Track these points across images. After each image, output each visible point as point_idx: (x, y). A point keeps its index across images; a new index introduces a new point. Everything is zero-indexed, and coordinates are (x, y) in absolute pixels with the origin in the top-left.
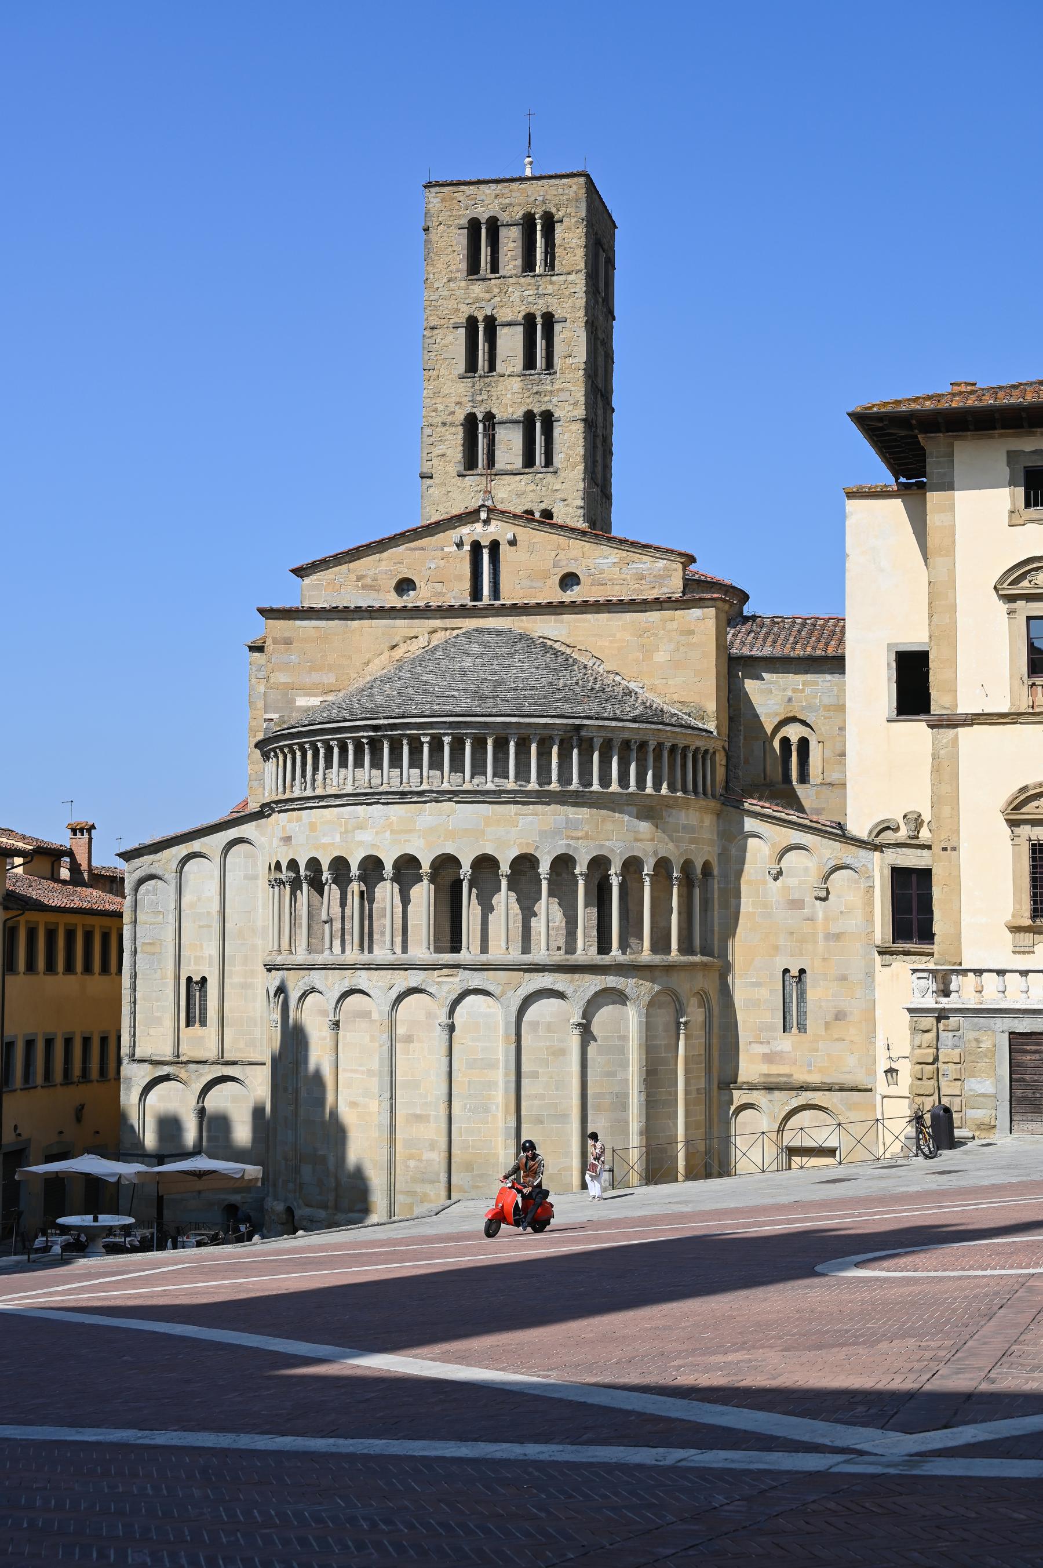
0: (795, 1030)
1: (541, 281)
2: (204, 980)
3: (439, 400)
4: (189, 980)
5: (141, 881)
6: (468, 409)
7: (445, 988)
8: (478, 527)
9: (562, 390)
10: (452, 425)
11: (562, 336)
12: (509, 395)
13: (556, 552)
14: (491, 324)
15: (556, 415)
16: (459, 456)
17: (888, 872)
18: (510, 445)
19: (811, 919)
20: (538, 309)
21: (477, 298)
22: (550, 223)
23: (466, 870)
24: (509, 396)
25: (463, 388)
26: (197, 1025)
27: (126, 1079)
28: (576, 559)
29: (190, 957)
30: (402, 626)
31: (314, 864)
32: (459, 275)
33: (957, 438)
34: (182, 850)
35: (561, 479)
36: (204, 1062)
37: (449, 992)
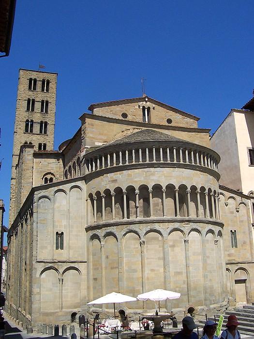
0: (234, 247)
2: (62, 233)
4: (57, 233)
5: (40, 198)
6: (27, 118)
7: (187, 228)
8: (144, 103)
12: (37, 117)
14: (34, 101)
16: (24, 129)
18: (36, 128)
21: (31, 95)
22: (48, 82)
23: (189, 189)
25: (26, 114)
26: (59, 249)
27: (35, 268)
28: (171, 115)
29: (57, 225)
30: (125, 127)
34: (56, 188)
36: (64, 262)
37: (188, 230)
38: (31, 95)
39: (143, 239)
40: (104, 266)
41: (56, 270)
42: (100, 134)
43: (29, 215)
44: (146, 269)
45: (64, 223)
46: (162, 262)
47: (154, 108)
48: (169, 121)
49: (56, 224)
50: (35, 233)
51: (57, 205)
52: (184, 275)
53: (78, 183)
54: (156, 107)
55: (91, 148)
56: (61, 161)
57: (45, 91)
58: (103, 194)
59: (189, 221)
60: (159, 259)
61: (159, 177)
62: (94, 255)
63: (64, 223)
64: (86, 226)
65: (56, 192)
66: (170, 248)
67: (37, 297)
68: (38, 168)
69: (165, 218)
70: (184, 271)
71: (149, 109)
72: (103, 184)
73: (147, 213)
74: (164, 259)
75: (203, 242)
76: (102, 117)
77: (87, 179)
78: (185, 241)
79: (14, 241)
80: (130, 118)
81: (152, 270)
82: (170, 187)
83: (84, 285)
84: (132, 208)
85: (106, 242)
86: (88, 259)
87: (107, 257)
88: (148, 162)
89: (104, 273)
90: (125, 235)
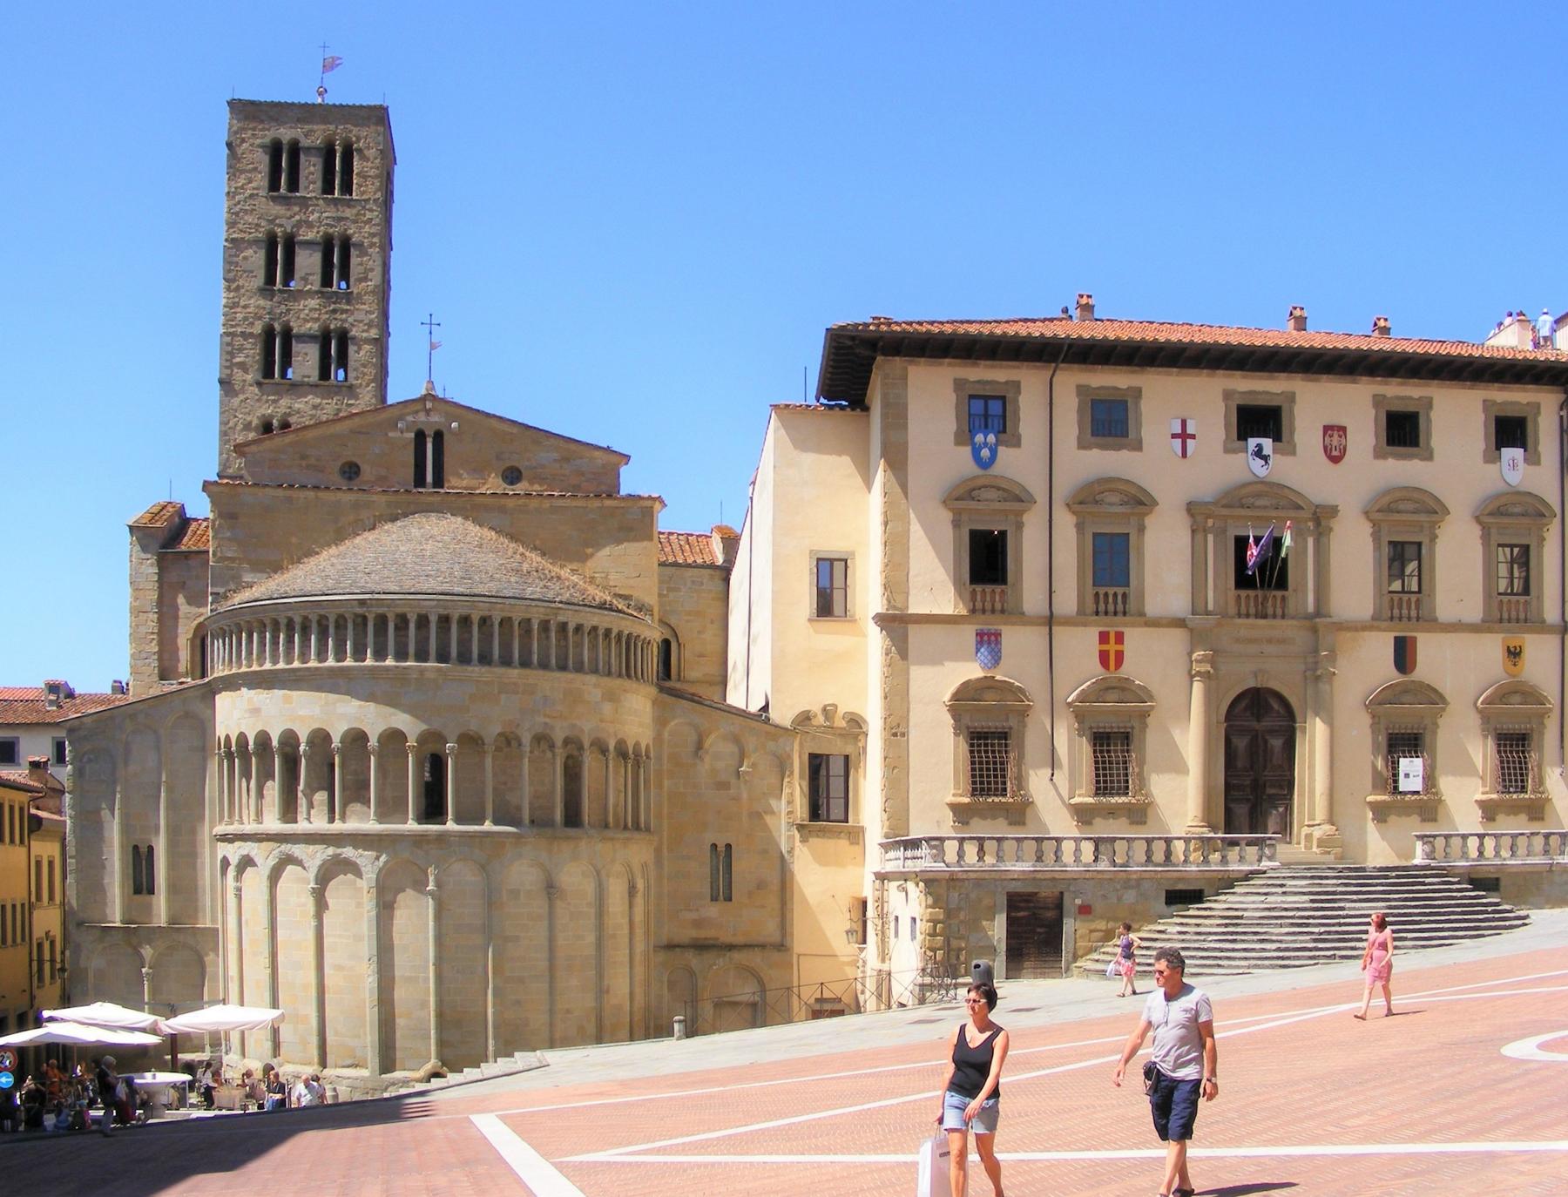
14: (290, 245)
17: (806, 757)
19: (737, 799)
20: (336, 231)
21: (284, 218)
31: (289, 738)
33: (911, 363)
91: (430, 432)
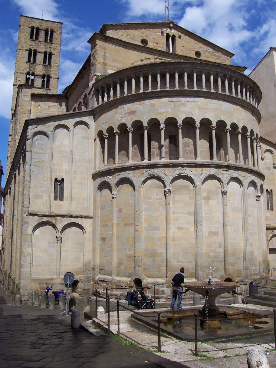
0: (269, 209)
1: (49, 44)
3: (20, 67)
4: (56, 179)
6: (28, 70)
7: (225, 176)
8: (169, 30)
9: (53, 70)
10: (23, 73)
11: (54, 58)
12: (39, 70)
13: (194, 44)
14: (36, 52)
15: (51, 76)
19: (273, 174)
20: (48, 50)
21: (33, 45)
22: (52, 32)
23: (228, 127)
24: (39, 69)
25: (27, 66)
30: (144, 56)
32: (28, 38)
34: (57, 123)
35: (51, 92)
38: (33, 45)
39: (169, 187)
40: (115, 221)
41: (54, 226)
42: (114, 60)
43: (21, 160)
44: (171, 226)
45: (66, 166)
46: (192, 219)
47: (180, 37)
48: (198, 54)
49: (55, 167)
50: (27, 178)
51: (57, 143)
52: (221, 236)
53: (85, 119)
54: (183, 36)
55: (101, 76)
56: (64, 105)
57: (48, 41)
58: (116, 130)
59: (228, 167)
60: (189, 213)
61: (192, 108)
62: (102, 208)
63: (66, 166)
64: (93, 172)
65: (56, 128)
66: (203, 201)
67: (28, 259)
68: (37, 111)
69: (199, 160)
70: (221, 231)
71: (174, 37)
72: (117, 117)
73: (174, 153)
74: (196, 214)
75: (245, 196)
76: (117, 39)
77: (95, 114)
78: (223, 193)
79: (9, 199)
80: (150, 45)
81: (180, 228)
82: (206, 123)
83: (88, 247)
84: (154, 148)
85: (118, 191)
86: (95, 213)
87: (120, 211)
88: (177, 88)
89: (115, 230)
90: (144, 182)
91: (171, 35)
